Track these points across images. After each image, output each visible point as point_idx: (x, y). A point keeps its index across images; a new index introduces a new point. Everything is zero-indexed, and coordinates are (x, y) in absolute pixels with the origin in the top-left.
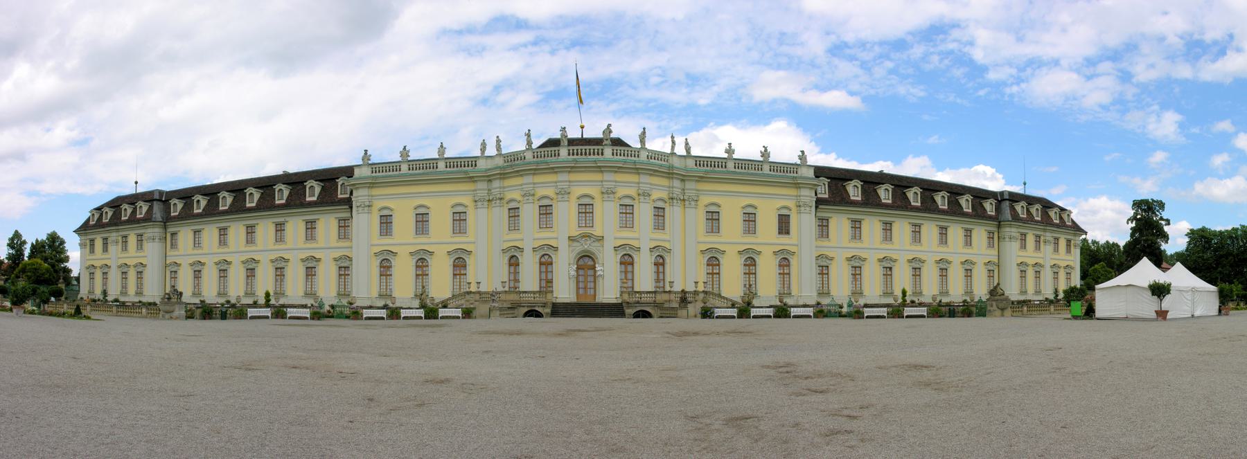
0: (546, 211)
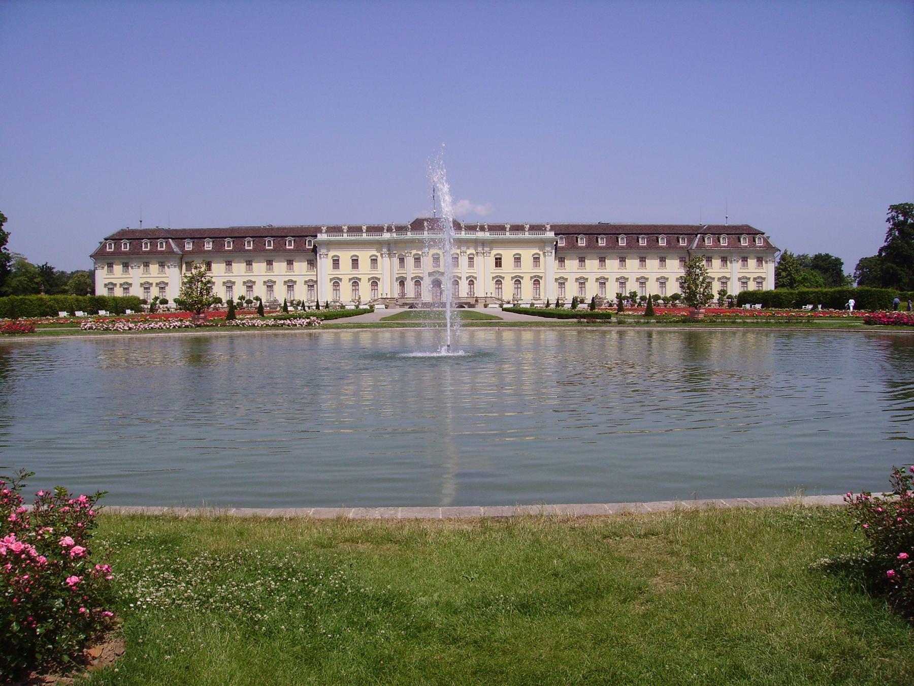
0: (417, 260)
